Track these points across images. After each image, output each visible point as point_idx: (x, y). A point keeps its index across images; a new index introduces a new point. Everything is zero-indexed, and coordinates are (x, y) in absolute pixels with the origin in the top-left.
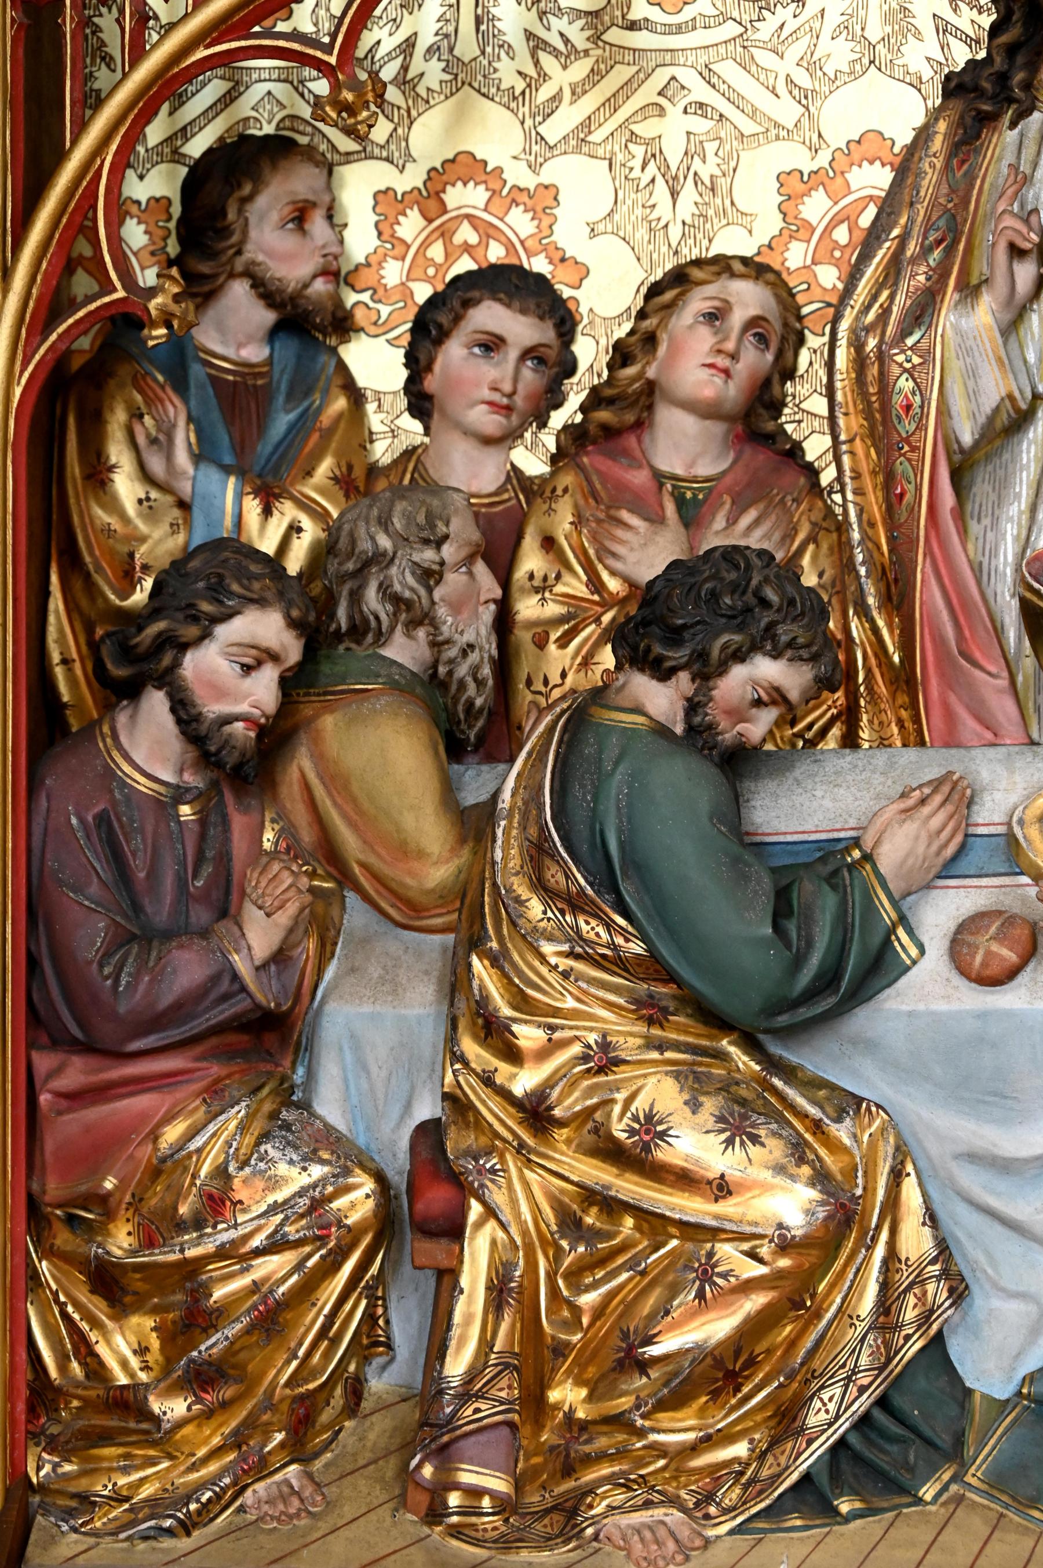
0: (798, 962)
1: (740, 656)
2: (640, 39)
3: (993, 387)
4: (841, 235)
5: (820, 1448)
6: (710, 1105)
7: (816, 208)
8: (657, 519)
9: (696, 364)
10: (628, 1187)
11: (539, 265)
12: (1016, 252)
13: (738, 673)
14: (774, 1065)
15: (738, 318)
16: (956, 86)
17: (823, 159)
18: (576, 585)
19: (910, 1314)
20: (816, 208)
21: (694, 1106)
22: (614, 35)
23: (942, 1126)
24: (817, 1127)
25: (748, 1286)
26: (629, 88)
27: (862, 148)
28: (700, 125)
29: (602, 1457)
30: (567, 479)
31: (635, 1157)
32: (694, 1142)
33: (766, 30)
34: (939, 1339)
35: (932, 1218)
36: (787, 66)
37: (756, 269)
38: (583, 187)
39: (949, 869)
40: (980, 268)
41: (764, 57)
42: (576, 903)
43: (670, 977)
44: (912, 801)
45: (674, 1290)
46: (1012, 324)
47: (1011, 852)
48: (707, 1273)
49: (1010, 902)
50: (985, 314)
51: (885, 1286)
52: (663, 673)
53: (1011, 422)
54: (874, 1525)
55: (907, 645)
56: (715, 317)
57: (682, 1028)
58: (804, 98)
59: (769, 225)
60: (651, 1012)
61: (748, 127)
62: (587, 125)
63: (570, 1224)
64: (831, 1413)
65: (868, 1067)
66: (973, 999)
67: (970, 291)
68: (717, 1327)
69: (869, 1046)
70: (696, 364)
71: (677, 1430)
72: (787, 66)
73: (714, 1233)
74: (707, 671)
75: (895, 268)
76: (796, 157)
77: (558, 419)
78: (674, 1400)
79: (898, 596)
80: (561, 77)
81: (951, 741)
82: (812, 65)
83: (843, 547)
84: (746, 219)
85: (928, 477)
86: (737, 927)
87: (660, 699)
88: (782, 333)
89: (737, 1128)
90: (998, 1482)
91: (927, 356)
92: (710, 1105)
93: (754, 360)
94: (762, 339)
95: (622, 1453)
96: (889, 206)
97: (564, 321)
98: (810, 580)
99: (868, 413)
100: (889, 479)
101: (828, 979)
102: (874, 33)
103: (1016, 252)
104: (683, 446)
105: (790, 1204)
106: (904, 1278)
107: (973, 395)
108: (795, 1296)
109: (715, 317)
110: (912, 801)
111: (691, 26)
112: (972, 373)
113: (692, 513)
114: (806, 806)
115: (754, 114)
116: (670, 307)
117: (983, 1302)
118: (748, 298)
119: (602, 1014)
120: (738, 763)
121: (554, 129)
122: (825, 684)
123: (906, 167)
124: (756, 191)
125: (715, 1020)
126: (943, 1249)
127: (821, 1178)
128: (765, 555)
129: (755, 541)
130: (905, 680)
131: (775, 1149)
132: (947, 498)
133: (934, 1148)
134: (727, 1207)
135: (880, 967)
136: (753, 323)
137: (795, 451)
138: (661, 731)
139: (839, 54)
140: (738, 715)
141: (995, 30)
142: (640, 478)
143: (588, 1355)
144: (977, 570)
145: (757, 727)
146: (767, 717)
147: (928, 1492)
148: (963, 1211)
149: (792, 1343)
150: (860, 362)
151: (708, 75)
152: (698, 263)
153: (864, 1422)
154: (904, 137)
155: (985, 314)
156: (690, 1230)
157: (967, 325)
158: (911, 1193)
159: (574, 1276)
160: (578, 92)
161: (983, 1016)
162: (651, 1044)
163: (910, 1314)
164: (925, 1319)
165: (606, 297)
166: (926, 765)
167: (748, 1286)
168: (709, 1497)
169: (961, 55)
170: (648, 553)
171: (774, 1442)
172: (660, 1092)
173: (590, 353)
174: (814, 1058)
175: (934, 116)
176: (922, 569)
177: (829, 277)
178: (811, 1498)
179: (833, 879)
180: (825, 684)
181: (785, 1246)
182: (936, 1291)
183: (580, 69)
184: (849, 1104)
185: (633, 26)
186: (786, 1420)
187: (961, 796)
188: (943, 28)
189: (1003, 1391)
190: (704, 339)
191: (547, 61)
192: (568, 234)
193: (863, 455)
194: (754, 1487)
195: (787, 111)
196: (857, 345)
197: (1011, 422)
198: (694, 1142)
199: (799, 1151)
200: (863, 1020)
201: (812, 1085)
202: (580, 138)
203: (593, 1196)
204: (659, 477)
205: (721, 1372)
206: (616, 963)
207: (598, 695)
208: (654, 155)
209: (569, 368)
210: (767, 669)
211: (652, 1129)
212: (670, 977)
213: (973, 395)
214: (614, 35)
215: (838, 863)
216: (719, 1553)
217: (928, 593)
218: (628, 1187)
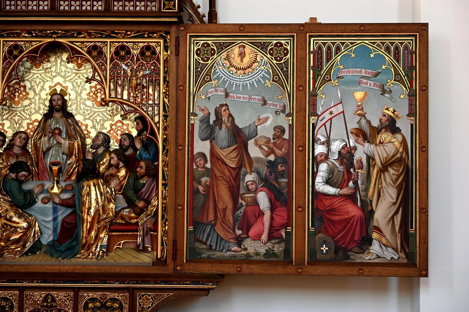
0: (26, 201)
1: (21, 171)
2: (13, 109)
3: (47, 145)
4: (33, 129)
5: (27, 249)
6: (17, 215)
7: (31, 126)
8: (13, 157)
9: (18, 142)
10: (9, 223)
11: (2, 131)
12: (49, 132)
13: (21, 173)
14: (24, 211)
15: (22, 137)
16: (45, 115)
17: (31, 122)
18: (5, 164)
19: (36, 236)
20: (31, 126)
21: (15, 215)
22: (11, 108)
23: (40, 218)
24: (28, 217)
25: (21, 233)
26: (12, 114)
27: (36, 121)
28: (19, 118)
29: (6, 250)
30: (5, 153)
31: (10, 220)
32: (15, 219)
33: (26, 109)
34: (39, 239)
35: (39, 226)
36: (28, 112)
37: (24, 132)
38: (7, 124)
39: (42, 193)
40: (46, 134)
41: (26, 111)
42: (4, 195)
43: (13, 202)
44: (38, 186)
45: (13, 233)
46: (49, 139)
47: (48, 191)
48: (16, 231)
49: (47, 196)
50: (46, 138)
51: (34, 233)
52: (13, 173)
53: (49, 149)
54: (32, 256)
55: (38, 171)
56: (20, 137)
57: (14, 208)
58: (30, 115)
59: (26, 128)
60: (11, 206)
61: (24, 118)
62: (8, 117)
63: (3, 227)
64: (29, 245)
65: (33, 212)
66: (43, 205)
67: (45, 136)
68: (17, 237)
69: (33, 210)
70: (18, 142)
71: (13, 247)
72: (28, 112)
73: (17, 227)
74: (18, 173)
75: (37, 134)
76: (29, 121)
77: (4, 147)
78: (13, 244)
79: (37, 166)
80: (5, 112)
81: (43, 180)
82: (30, 112)
83: (32, 160)
84: (24, 127)
85: (41, 154)
86: (20, 198)
87: (13, 175)
88: (27, 139)
89: (19, 217)
90: (44, 252)
91: (41, 142)
92: (17, 215)
93: (24, 142)
94: (25, 140)
95: (8, 249)
96: (38, 126)
97: (5, 137)
98: (29, 164)
99: (35, 147)
100: (37, 154)
101: (29, 203)
102: (37, 109)
103: (49, 132)
104: (16, 150)
105: (25, 225)
106: (36, 232)
107: (45, 146)
108: (25, 234)
109: (20, 137)
110: (38, 186)
111: (18, 108)
112: (45, 144)
113: (17, 157)
114: (28, 186)
115: (25, 117)
116: (15, 136)
117: (44, 235)
118: (23, 136)
119: (7, 206)
120: (21, 182)
121: (4, 118)
122: (29, 175)
123: (40, 122)
124: (25, 124)
125: (18, 207)
126: (40, 230)
127: (28, 222)
128: (24, 162)
129: (23, 160)
130: (38, 174)
131: (23, 219)
132: (43, 156)
133: (39, 220)
134: (18, 225)
135: (34, 202)
136: (24, 138)
137: (28, 151)
138: (13, 179)
139: (33, 111)
140: (21, 177)
141: (49, 110)
142: (12, 153)
143: (5, 239)
144: (45, 163)
145: (23, 178)
146: (24, 178)
147: (38, 253)
148: (42, 226)
149: (25, 238)
150: (34, 142)
151: (20, 113)
152: (19, 132)
153: (31, 246)
154: (40, 120)
155: (46, 138)
156: (15, 227)
157: (45, 139)
158: (37, 224)
159: (4, 232)
160: (7, 114)
161: (44, 207)
162: (11, 209)
163: (36, 236)
164: (38, 236)
165: (9, 134)
166: (40, 182)
167: (21, 233)
168: (16, 254)
169: (46, 112)
170: (13, 161)
171: (23, 248)
172: (12, 214)
173: (7, 140)
174: (27, 211)
175: (43, 118)
176: (40, 163)
177: (32, 133)
178: (26, 254)
179: (30, 194)
180: (29, 175)
181: (24, 229)
182: (39, 234)
183: (7, 112)
184: (31, 215)
185: (13, 107)
186: (24, 246)
187: (43, 186)
188: (44, 109)
189: (45, 244)
190: (19, 140)
191: (4, 111)
192: (6, 128)
193: (35, 152)
194: (21, 253)
195: (28, 117)
196: (34, 141)
197: (49, 149)
198: (15, 219)
199: (26, 220)
200: (32, 207)
201: (27, 213)
202: (7, 119)
203: (5, 224)
204: (14, 153)
205: (17, 241)
206: (8, 201)
207: (7, 175)
208: (14, 120)
209: (6, 141)
210: (24, 173)
211: (11, 217)
212: (13, 202)
213: (45, 146)
214: (11, 108)
215: (30, 192)
216: (17, 259)
217: (40, 165)
218: (9, 223)
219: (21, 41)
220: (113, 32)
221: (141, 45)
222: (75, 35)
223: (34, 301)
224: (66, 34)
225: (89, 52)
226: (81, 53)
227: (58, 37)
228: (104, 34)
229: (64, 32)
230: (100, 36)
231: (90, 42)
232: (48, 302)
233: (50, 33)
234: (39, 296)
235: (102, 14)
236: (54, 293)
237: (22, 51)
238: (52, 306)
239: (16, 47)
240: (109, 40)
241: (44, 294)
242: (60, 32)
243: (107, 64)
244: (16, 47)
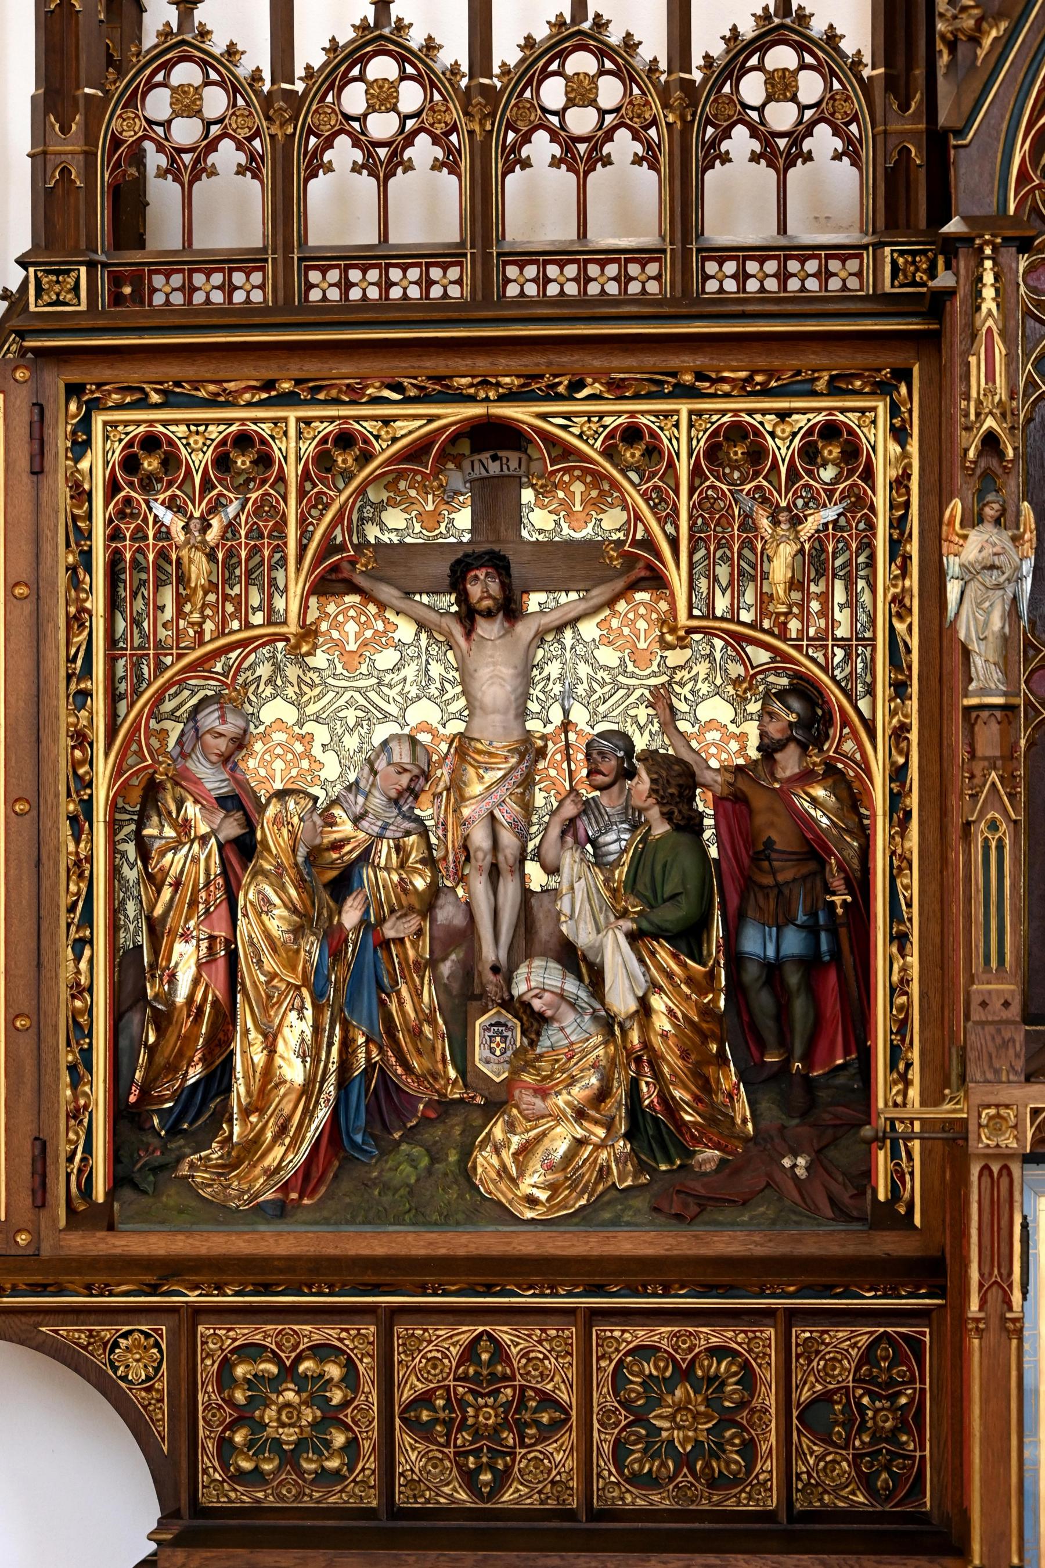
219: (364, 420)
220: (700, 376)
221: (800, 421)
222: (561, 389)
223: (428, 1360)
224: (529, 384)
225: (609, 453)
226: (585, 458)
227: (501, 399)
228: (668, 383)
229: (522, 381)
230: (654, 389)
231: (617, 413)
232: (479, 1363)
233: (471, 385)
234: (450, 1340)
235: (666, 310)
236: (504, 1333)
237: (366, 457)
238: (493, 1378)
239: (345, 440)
240: (684, 408)
241: (467, 1332)
242: (507, 380)
243: (677, 492)
244: (345, 440)
